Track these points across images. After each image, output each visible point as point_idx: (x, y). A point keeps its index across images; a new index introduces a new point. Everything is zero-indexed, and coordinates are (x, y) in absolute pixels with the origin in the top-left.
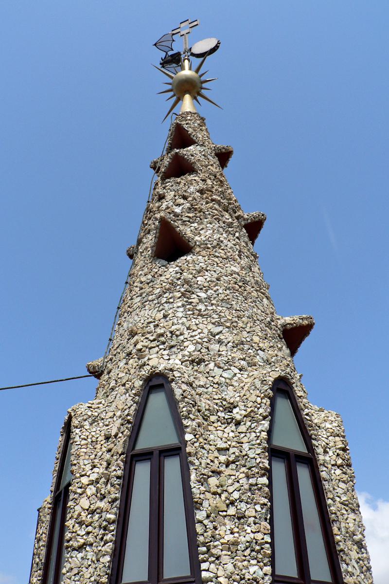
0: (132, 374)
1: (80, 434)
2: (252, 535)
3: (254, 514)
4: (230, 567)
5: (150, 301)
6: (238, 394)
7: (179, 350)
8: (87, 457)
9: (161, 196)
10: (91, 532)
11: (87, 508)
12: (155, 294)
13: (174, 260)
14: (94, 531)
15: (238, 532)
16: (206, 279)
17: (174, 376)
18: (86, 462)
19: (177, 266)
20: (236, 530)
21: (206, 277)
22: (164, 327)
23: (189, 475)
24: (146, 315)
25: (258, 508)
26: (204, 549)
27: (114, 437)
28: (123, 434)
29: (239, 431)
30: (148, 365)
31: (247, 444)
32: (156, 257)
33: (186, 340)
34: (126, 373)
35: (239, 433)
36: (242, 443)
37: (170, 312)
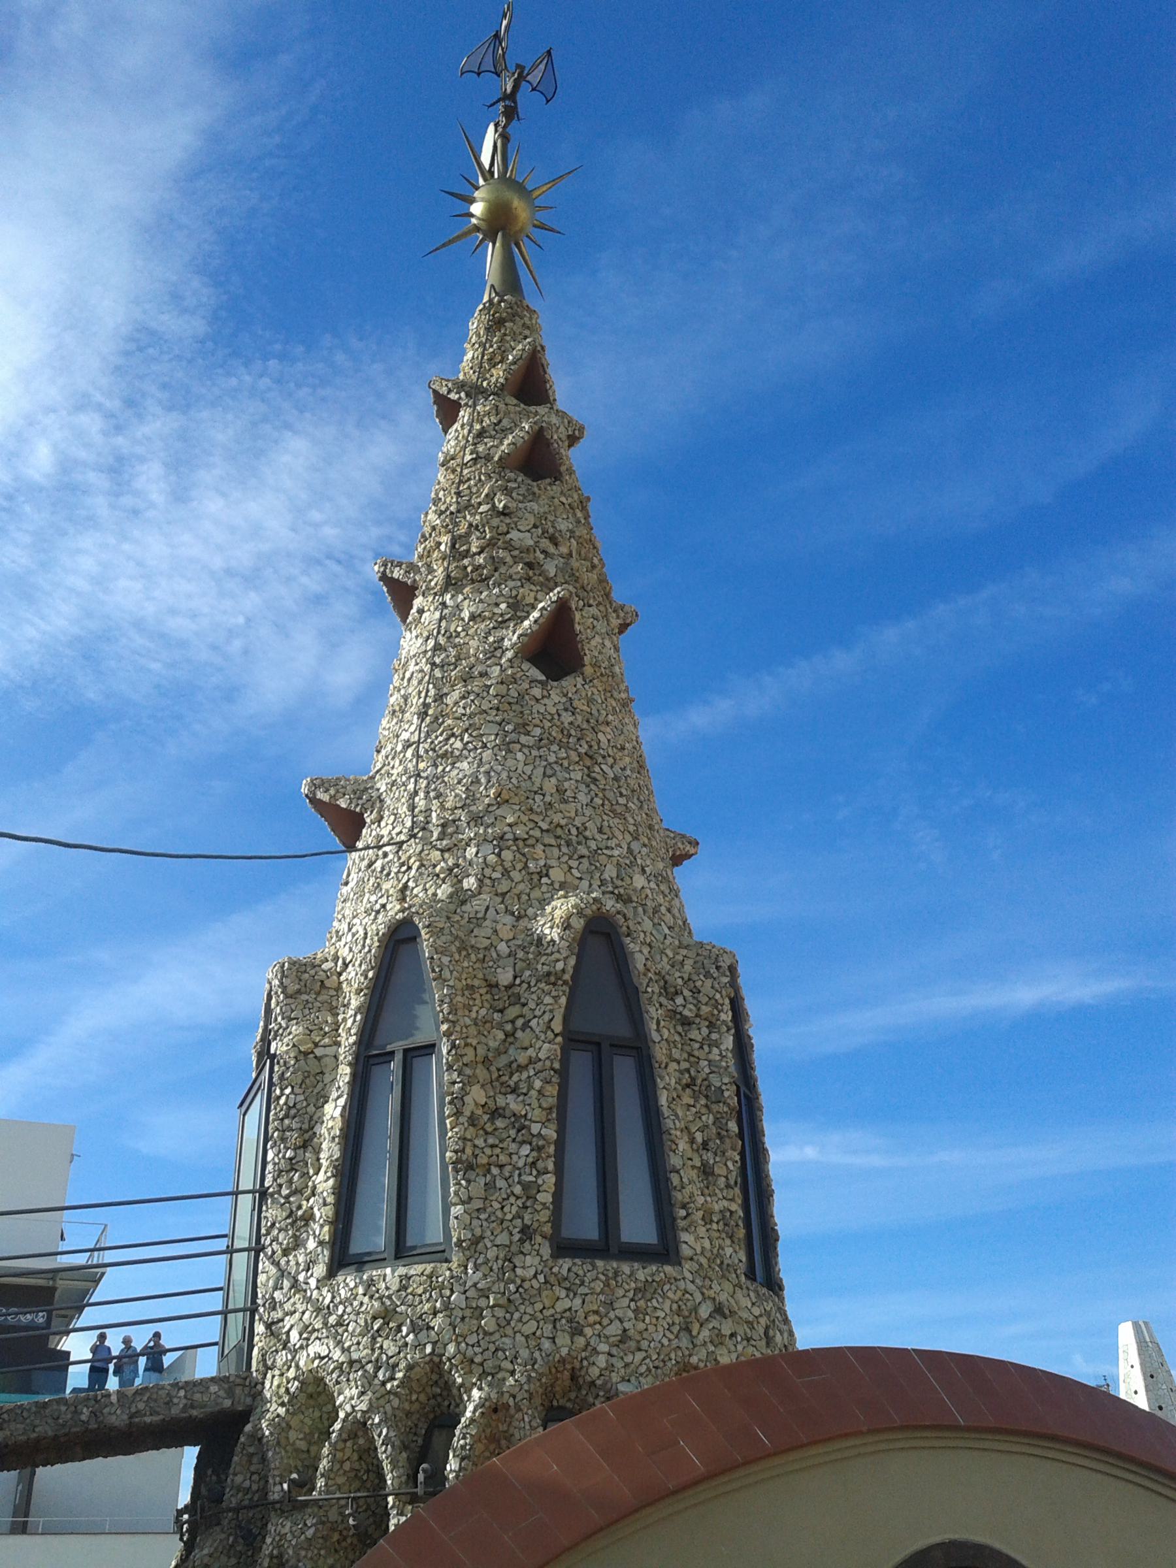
0: (516, 880)
1: (452, 968)
2: (725, 1203)
3: (724, 1172)
4: (707, 1244)
5: (523, 746)
6: (679, 975)
7: (593, 867)
8: (467, 1013)
9: (507, 511)
10: (497, 1146)
11: (483, 1103)
12: (533, 737)
13: (557, 678)
14: (501, 1146)
15: (710, 1195)
16: (609, 740)
17: (628, 928)
18: (468, 1021)
19: (565, 695)
20: (706, 1191)
21: (609, 737)
22: (561, 812)
23: (656, 1100)
24: (519, 771)
25: (730, 1164)
26: (683, 1213)
27: (503, 989)
28: (556, 1001)
29: (693, 1037)
30: (547, 875)
31: (706, 1063)
32: (520, 655)
33: (599, 851)
34: (503, 875)
35: (691, 1040)
36: (698, 1058)
37: (566, 785)
